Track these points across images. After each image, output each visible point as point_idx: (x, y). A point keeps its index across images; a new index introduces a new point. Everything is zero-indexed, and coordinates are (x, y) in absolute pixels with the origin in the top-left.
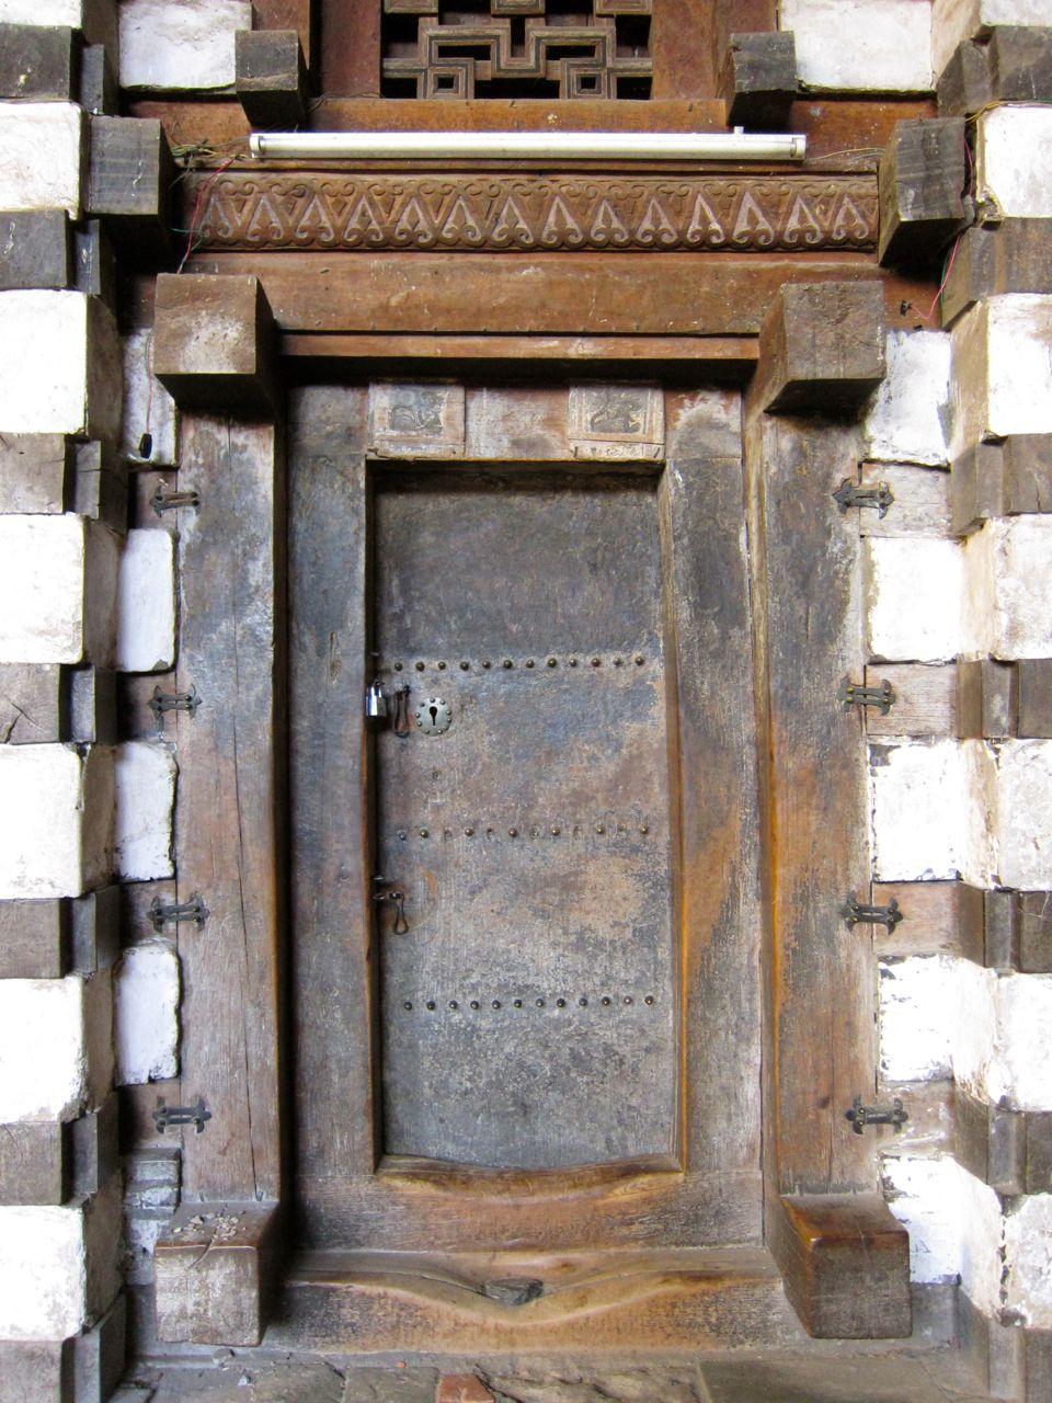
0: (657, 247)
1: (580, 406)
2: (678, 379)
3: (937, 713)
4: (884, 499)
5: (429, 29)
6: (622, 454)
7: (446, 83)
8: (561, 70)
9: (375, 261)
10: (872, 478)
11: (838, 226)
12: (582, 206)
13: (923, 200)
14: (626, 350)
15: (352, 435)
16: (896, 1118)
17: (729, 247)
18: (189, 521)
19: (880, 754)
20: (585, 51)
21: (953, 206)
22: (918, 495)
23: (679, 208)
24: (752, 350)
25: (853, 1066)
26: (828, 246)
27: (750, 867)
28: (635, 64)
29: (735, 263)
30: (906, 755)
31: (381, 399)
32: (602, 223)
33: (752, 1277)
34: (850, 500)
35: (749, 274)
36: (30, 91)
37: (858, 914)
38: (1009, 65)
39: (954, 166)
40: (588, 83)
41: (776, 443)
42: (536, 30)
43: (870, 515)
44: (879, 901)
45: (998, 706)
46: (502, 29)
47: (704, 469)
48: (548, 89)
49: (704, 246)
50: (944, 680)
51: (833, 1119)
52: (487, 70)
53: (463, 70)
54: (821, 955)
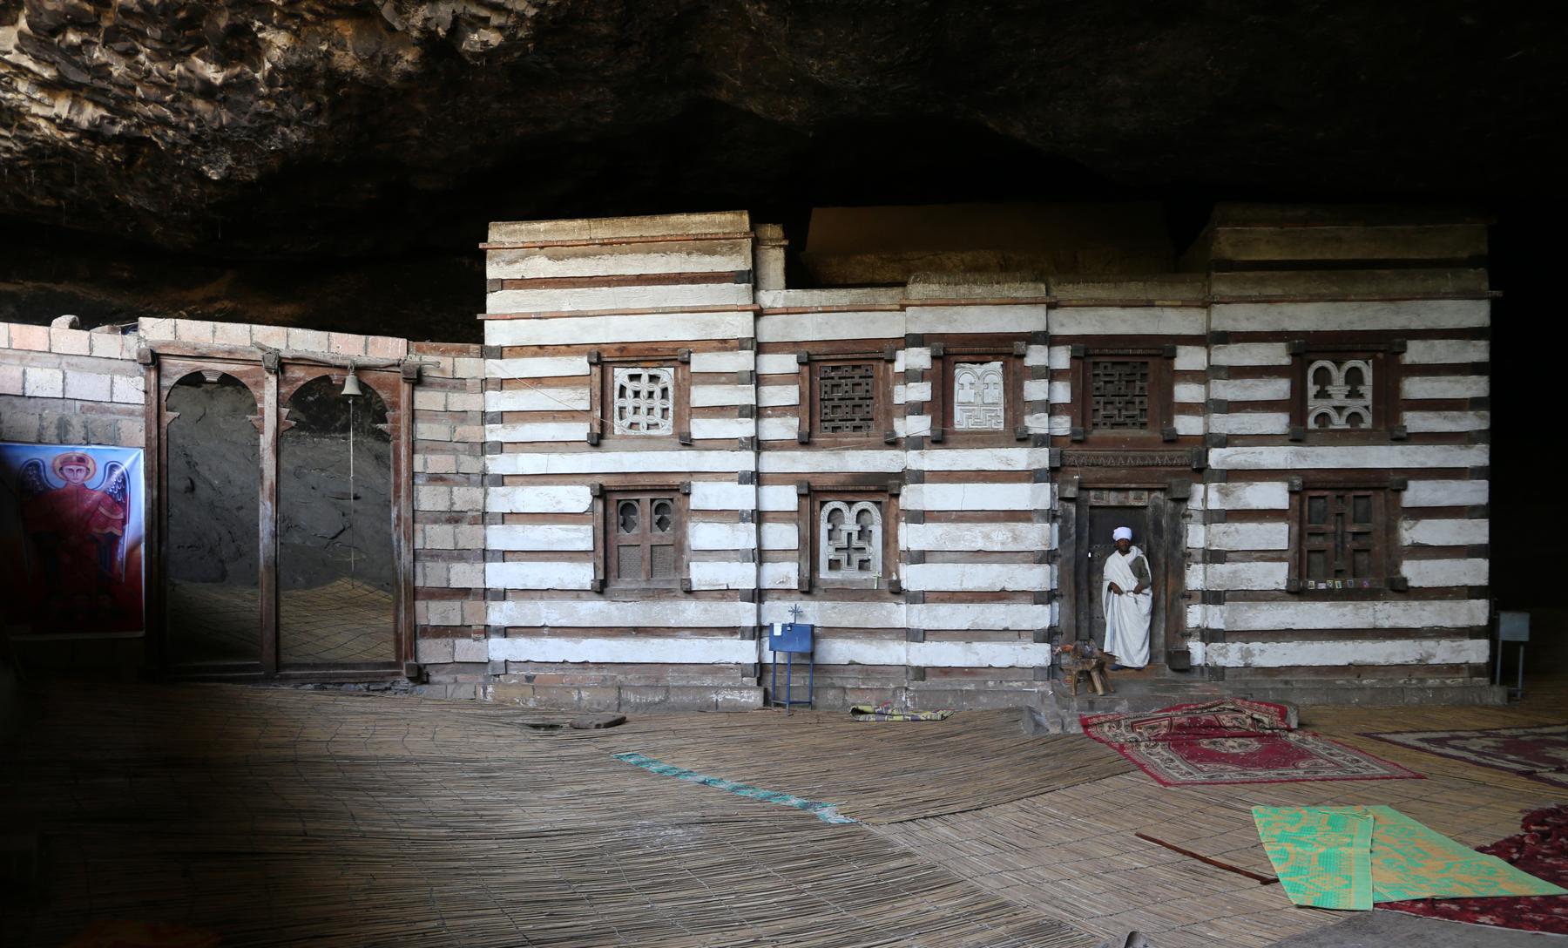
0: (1149, 466)
1: (1132, 494)
2: (1151, 490)
3: (1199, 558)
4: (1191, 516)
5: (1102, 412)
6: (1140, 504)
7: (1105, 424)
8: (1128, 421)
9: (1094, 469)
10: (1188, 513)
11: (1184, 462)
12: (1134, 458)
13: (1198, 464)
14: (1142, 486)
15: (1086, 501)
16: (1190, 635)
17: (1163, 466)
18: (1060, 520)
19: (1189, 566)
20: (1133, 417)
21: (1204, 466)
22: (1199, 516)
23: (1153, 458)
24: (1166, 486)
25: (1182, 626)
26: (1181, 466)
27: (1163, 588)
28: (1144, 420)
29: (1163, 469)
30: (1194, 566)
31: (1092, 493)
32: (1138, 462)
33: (1163, 666)
34: (1184, 516)
35: (1167, 471)
36: (1041, 446)
37: (1184, 596)
38: (1215, 440)
39: (1204, 457)
40: (1134, 424)
41: (1171, 505)
42: (1124, 412)
43: (1188, 519)
44: (1187, 594)
45: (1208, 557)
46: (1116, 412)
47: (1156, 507)
48: (1125, 424)
49: (1157, 465)
50: (1201, 552)
51: (1178, 636)
52: (1113, 421)
53: (1108, 421)
54: (1176, 604)
